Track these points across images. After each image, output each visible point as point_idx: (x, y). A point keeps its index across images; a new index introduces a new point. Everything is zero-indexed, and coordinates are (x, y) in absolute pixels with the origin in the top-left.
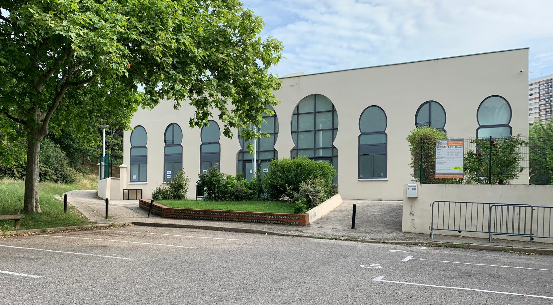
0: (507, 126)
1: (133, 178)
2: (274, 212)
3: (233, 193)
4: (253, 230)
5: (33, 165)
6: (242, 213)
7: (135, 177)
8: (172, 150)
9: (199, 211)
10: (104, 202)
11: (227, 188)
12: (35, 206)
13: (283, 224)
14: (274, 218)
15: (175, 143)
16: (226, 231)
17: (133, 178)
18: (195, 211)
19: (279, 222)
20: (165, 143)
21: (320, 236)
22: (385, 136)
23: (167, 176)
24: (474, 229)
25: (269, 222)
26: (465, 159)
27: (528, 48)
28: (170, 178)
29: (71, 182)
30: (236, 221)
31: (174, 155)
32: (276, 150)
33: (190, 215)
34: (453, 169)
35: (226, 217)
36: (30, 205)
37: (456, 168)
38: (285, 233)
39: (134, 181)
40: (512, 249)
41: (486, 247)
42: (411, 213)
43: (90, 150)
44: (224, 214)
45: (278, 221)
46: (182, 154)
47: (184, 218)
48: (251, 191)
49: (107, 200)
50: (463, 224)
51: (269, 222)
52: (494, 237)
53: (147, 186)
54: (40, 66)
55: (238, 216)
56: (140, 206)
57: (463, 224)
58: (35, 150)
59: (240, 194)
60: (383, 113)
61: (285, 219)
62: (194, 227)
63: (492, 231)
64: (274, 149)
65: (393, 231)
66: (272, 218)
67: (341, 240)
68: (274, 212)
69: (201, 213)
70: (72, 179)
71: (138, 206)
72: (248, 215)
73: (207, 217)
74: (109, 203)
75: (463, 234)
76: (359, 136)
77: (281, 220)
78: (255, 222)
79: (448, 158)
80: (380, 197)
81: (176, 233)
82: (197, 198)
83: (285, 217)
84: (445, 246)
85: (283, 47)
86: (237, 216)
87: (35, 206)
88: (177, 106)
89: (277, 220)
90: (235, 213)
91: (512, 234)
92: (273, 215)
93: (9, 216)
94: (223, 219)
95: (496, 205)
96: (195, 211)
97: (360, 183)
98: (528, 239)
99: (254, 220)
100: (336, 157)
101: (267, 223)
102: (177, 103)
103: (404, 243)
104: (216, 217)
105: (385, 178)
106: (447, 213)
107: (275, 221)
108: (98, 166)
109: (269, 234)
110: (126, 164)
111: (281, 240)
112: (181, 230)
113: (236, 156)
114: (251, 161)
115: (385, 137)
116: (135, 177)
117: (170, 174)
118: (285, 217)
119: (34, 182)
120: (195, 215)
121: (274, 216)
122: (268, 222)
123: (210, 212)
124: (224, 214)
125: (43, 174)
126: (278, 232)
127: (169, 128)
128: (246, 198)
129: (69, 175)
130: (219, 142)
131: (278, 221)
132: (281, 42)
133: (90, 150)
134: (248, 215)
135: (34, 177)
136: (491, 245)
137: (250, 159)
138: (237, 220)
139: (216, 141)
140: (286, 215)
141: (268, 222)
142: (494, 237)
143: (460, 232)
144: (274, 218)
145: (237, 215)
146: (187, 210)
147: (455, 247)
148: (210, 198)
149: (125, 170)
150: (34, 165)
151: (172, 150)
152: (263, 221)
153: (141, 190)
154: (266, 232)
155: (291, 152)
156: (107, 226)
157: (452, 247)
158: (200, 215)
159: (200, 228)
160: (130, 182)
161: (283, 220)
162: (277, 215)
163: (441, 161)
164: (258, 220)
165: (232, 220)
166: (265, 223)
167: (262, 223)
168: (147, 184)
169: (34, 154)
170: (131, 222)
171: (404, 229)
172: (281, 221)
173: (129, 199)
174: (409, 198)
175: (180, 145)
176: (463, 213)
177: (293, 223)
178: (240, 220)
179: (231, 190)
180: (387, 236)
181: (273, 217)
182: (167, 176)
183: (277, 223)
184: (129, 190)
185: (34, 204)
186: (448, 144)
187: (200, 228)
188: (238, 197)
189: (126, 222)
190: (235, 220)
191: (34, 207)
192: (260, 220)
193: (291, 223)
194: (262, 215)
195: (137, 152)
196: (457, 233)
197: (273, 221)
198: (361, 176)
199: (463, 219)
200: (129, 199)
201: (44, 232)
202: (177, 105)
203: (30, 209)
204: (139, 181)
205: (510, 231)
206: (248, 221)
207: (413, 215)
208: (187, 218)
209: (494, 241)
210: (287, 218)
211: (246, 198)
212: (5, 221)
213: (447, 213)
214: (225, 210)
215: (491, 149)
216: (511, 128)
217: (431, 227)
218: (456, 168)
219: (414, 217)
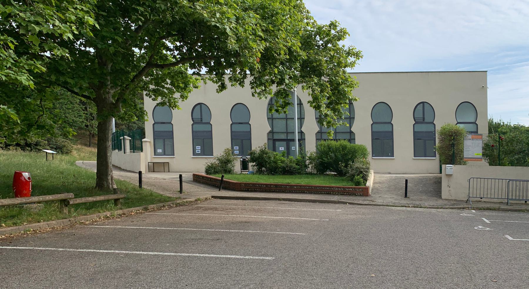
0: (475, 123)
1: (158, 152)
2: (339, 185)
3: (284, 168)
4: (335, 201)
5: (106, 142)
6: (312, 186)
7: (159, 151)
8: (200, 128)
9: (271, 185)
10: (138, 175)
11: (276, 164)
12: (111, 183)
13: (349, 195)
14: (341, 190)
15: (203, 121)
16: (310, 202)
17: (158, 152)
18: (266, 185)
19: (345, 193)
20: (193, 121)
21: (391, 204)
22: (391, 126)
23: (197, 150)
24: (489, 196)
25: (337, 193)
26: (483, 149)
27: (487, 71)
28: (200, 152)
29: (67, 153)
30: (306, 193)
31: (204, 132)
32: (303, 132)
33: (261, 188)
34: (476, 155)
35: (297, 189)
36: (105, 183)
37: (478, 154)
38: (361, 202)
39: (158, 154)
40: (526, 210)
41: (510, 209)
42: (448, 186)
43: (78, 121)
44: (295, 187)
45: (344, 192)
46: (211, 131)
47: (251, 191)
48: (298, 167)
49: (140, 173)
50: (482, 193)
51: (337, 193)
52: (510, 201)
53: (174, 159)
54: (232, 59)
55: (308, 189)
56: (193, 179)
57: (482, 193)
58: (108, 127)
59: (290, 169)
60: (390, 108)
61: (350, 190)
62: (279, 199)
63: (510, 197)
64: (301, 131)
65: (424, 197)
66: (339, 190)
67: (409, 207)
68: (339, 185)
69: (272, 186)
70: (68, 150)
71: (192, 180)
72: (318, 188)
73: (278, 190)
74: (143, 176)
75: (483, 200)
76: (372, 125)
77: (347, 192)
78: (324, 193)
79: (472, 147)
80: (389, 171)
81: (271, 206)
82: (241, 172)
83: (351, 189)
84: (484, 209)
85: (363, 56)
86: (307, 189)
87: (111, 183)
88: (254, 94)
89: (343, 192)
90: (306, 187)
91: (515, 200)
92: (340, 188)
93: (112, 195)
94: (268, 190)
95: (513, 180)
96: (266, 184)
97: (374, 160)
98: (524, 202)
99: (323, 192)
100: (354, 140)
101: (335, 194)
102: (254, 91)
103: (460, 208)
104: (288, 190)
105: (392, 157)
106: (500, 187)
107: (342, 192)
108: (121, 140)
109: (350, 203)
110: (149, 138)
111: (357, 208)
112: (269, 202)
113: (266, 135)
114: (293, 140)
115: (391, 127)
116: (159, 151)
117: (200, 149)
118: (351, 189)
119: (109, 160)
120: (267, 188)
121: (341, 189)
122: (336, 194)
123: (281, 185)
124: (295, 187)
125: (34, 144)
126: (356, 202)
127: (196, 107)
128: (296, 173)
129: (64, 146)
130: (250, 123)
131: (344, 192)
132: (361, 51)
133: (78, 121)
134: (318, 188)
135: (108, 155)
136: (509, 208)
137: (292, 138)
138: (308, 192)
139: (246, 122)
140: (351, 188)
141: (336, 194)
142: (510, 201)
143: (481, 198)
144: (341, 190)
145: (307, 188)
146: (258, 184)
147: (490, 210)
148: (260, 172)
149: (148, 144)
150: (107, 143)
151: (200, 128)
152: (332, 193)
153: (168, 163)
154: (347, 203)
155: (316, 134)
156: (194, 200)
157: (488, 210)
158: (272, 188)
159: (284, 200)
160: (155, 155)
161: (349, 192)
162: (343, 188)
163: (467, 149)
164: (327, 192)
165: (303, 192)
166: (333, 194)
167: (330, 194)
168: (174, 157)
169: (107, 131)
170: (211, 196)
171: (443, 197)
172: (347, 193)
173: (154, 172)
174: (447, 175)
175: (209, 123)
176: (482, 185)
177: (358, 194)
178: (310, 192)
179: (282, 166)
180: (432, 203)
181: (340, 189)
182: (197, 150)
183: (344, 194)
184: (153, 163)
185: (110, 181)
186: (472, 137)
187: (284, 200)
188: (287, 171)
189: (208, 196)
190: (306, 192)
191: (110, 184)
192: (329, 192)
193: (356, 194)
194: (331, 188)
195: (160, 128)
196: (480, 199)
197: (341, 192)
198: (374, 155)
199: (482, 189)
200: (155, 171)
201: (146, 209)
202: (254, 92)
203: (106, 186)
204: (165, 155)
205: (514, 198)
206: (318, 192)
207: (450, 187)
208: (258, 191)
209: (512, 204)
210: (353, 190)
211: (296, 173)
212: (108, 201)
213: (500, 187)
214: (293, 183)
215: (499, 141)
216: (477, 125)
217: (468, 196)
218: (478, 154)
219: (451, 189)
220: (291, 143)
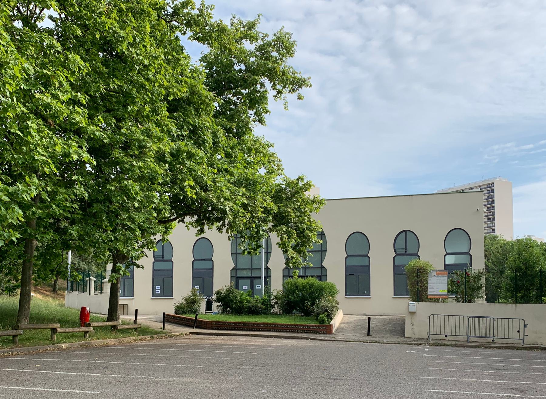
3: (249, 308)
6: (278, 325)
8: (161, 266)
14: (305, 328)
15: (165, 259)
19: (309, 332)
20: (154, 258)
31: (165, 270)
46: (172, 270)
50: (446, 331)
53: (133, 300)
57: (446, 331)
72: (283, 326)
83: (315, 328)
89: (308, 330)
92: (305, 326)
95: (472, 317)
118: (315, 328)
131: (308, 331)
134: (283, 326)
140: (315, 326)
148: (225, 312)
151: (161, 266)
162: (308, 326)
166: (297, 332)
167: (295, 332)
171: (407, 335)
174: (410, 312)
188: (253, 311)
196: (444, 337)
199: (446, 328)
214: (260, 322)
219: (414, 327)
220: (256, 281)
